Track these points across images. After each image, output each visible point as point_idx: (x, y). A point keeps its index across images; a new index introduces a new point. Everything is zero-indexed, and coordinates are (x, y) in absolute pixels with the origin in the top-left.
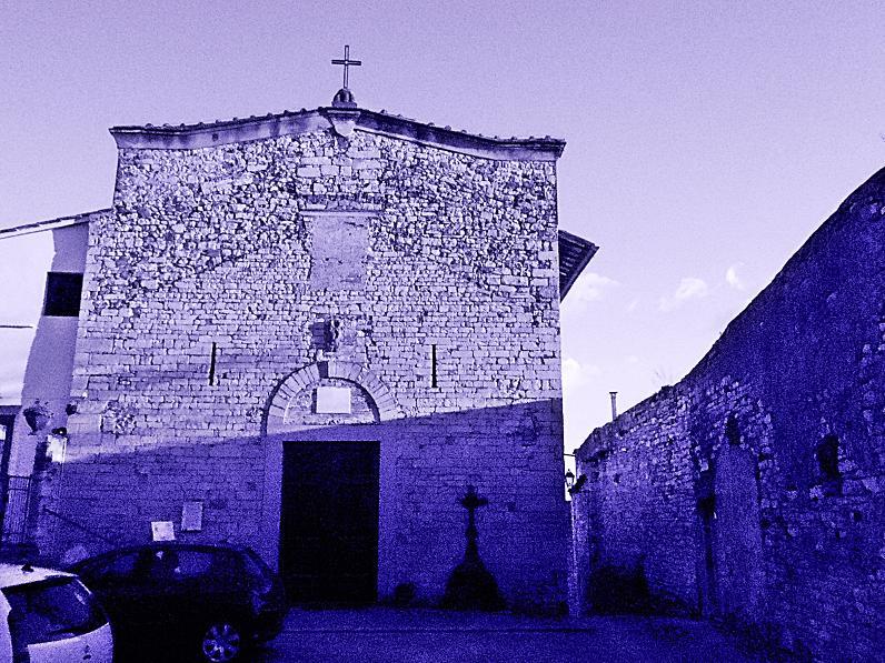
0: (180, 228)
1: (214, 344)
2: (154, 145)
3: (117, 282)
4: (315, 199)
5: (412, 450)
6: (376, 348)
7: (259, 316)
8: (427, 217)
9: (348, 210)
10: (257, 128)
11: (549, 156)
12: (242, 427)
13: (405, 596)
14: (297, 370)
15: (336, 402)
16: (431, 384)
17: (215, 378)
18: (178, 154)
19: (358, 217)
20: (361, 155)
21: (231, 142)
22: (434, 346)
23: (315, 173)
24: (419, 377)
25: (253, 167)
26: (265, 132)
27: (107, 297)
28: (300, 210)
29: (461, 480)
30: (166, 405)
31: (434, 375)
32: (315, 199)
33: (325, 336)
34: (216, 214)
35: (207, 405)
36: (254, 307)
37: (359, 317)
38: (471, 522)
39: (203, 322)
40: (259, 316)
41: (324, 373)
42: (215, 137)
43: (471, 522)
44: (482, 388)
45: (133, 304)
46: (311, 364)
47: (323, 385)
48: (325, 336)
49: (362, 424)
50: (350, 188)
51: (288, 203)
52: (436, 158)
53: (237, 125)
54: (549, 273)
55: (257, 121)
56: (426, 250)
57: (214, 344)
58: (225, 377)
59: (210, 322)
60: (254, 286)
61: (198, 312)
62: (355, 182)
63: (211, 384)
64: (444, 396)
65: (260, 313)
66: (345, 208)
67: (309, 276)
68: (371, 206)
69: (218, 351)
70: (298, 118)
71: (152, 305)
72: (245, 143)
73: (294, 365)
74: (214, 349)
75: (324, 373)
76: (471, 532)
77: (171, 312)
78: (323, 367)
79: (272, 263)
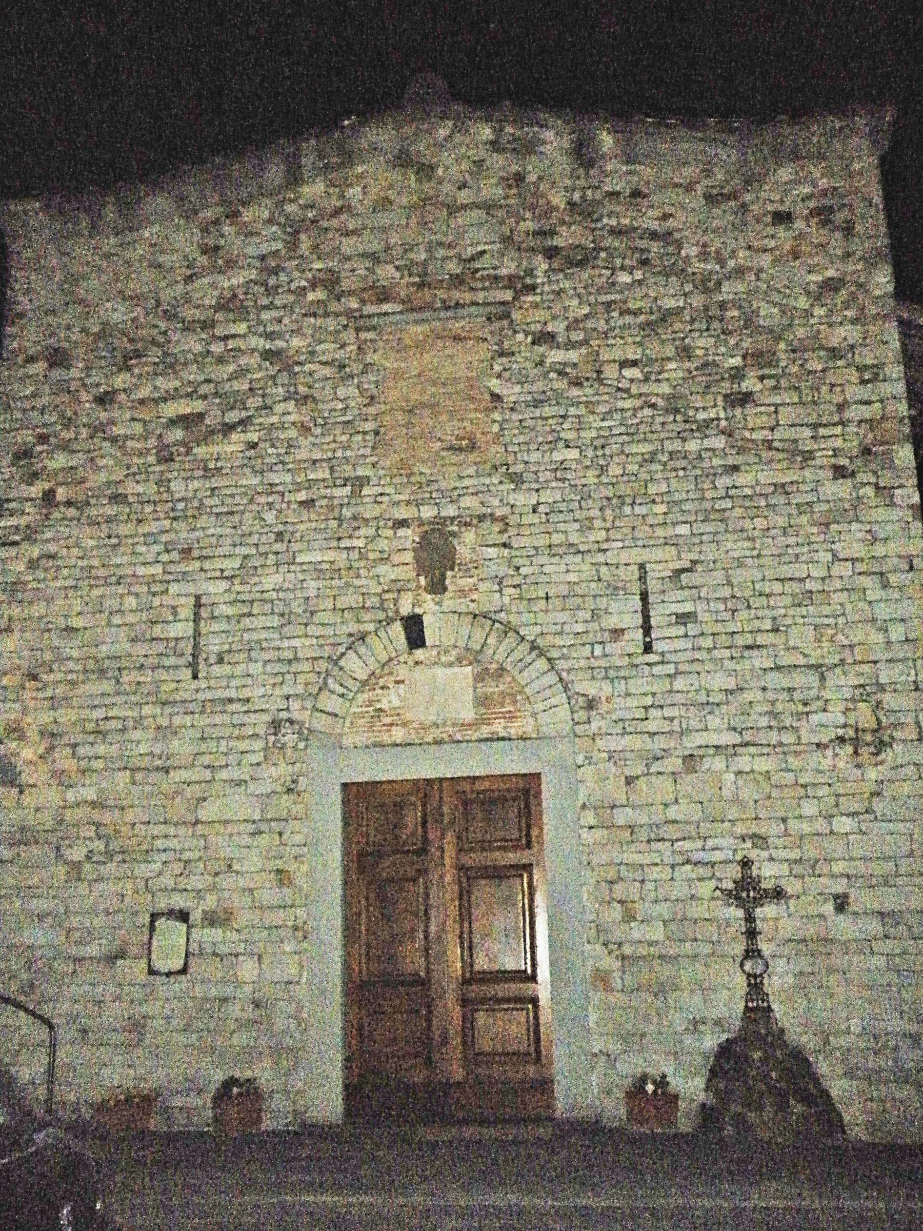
0: (121, 380)
1: (198, 598)
5: (616, 791)
7: (280, 536)
9: (447, 308)
14: (363, 637)
17: (202, 666)
20: (464, 197)
22: (642, 566)
24: (617, 633)
30: (114, 724)
35: (188, 720)
37: (481, 518)
39: (175, 556)
46: (390, 621)
49: (503, 739)
54: (887, 389)
56: (611, 372)
58: (220, 661)
59: (186, 552)
61: (164, 538)
65: (281, 527)
69: (204, 613)
73: (353, 628)
77: (114, 541)
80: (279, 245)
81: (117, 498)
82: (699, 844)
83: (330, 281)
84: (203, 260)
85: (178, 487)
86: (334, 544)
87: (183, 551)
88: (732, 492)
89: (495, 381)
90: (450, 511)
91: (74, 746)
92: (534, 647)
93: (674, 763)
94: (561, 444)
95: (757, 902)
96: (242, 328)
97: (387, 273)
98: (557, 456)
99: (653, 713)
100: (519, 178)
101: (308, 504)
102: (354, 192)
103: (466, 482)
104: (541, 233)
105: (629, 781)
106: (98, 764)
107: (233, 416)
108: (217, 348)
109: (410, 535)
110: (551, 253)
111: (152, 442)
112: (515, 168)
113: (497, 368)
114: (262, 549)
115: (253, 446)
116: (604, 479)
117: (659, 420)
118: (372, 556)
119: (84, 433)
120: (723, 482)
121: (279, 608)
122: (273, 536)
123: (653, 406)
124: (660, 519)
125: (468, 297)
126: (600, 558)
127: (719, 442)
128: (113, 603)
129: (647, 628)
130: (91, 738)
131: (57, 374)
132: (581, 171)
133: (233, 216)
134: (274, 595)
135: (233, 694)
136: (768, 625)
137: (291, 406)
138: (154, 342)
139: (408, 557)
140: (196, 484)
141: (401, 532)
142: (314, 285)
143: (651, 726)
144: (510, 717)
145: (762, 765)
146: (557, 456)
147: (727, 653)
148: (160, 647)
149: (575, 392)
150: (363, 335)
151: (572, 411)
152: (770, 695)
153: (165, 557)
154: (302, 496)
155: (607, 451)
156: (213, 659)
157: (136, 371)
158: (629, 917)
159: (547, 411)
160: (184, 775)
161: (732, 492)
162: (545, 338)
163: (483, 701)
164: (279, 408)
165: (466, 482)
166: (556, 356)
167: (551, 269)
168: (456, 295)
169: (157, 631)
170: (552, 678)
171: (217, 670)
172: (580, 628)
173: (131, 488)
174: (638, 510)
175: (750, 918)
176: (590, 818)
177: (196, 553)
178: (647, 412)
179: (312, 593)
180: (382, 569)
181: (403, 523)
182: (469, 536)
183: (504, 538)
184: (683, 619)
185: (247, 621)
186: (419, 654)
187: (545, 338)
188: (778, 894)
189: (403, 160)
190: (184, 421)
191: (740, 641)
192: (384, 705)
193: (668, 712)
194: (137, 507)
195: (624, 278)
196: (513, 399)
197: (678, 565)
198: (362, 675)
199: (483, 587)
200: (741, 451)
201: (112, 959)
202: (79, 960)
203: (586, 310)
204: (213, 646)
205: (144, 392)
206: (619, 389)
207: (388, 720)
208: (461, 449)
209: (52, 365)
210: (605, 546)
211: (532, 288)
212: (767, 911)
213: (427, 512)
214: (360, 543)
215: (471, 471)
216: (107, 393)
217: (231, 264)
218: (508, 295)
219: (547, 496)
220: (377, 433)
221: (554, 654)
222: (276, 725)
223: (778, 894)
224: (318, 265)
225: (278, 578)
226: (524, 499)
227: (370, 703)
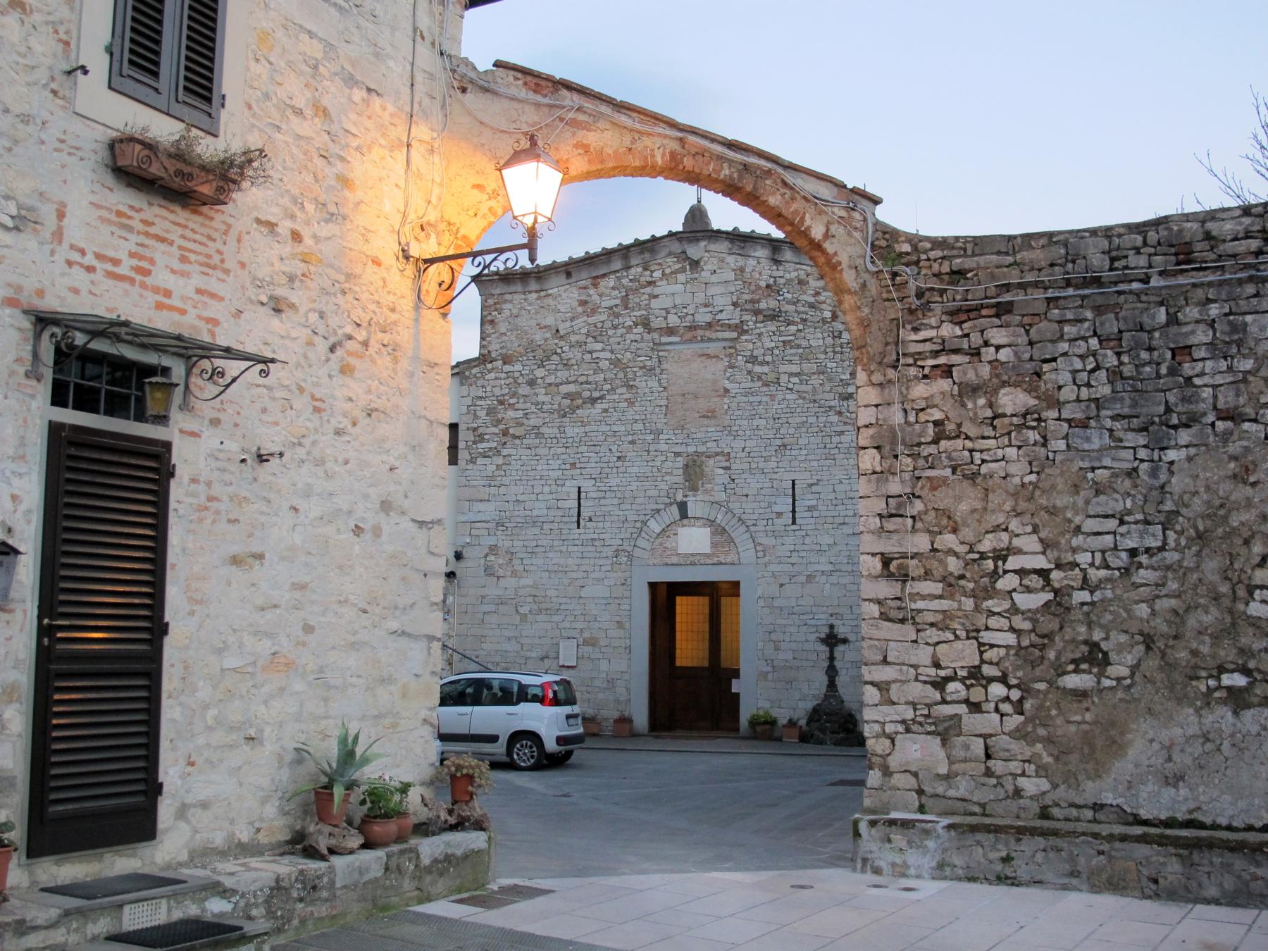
0: (540, 373)
1: (579, 488)
2: (512, 288)
3: (488, 431)
4: (671, 331)
5: (775, 589)
6: (734, 486)
8: (783, 342)
9: (702, 341)
10: (608, 262)
12: (609, 568)
13: (765, 729)
14: (658, 511)
15: (694, 539)
16: (790, 521)
17: (581, 521)
18: (535, 295)
19: (713, 348)
20: (714, 279)
21: (584, 276)
22: (793, 481)
23: (668, 303)
24: (779, 515)
25: (607, 303)
26: (617, 265)
27: (479, 445)
28: (654, 344)
29: (823, 619)
30: (539, 549)
31: (794, 511)
32: (671, 331)
33: (693, 472)
34: (574, 355)
36: (614, 448)
37: (717, 454)
38: (832, 658)
39: (568, 466)
40: (619, 458)
41: (684, 514)
42: (569, 275)
43: (832, 658)
44: (844, 523)
45: (505, 452)
46: (671, 504)
47: (683, 526)
48: (693, 472)
50: (703, 317)
51: (642, 338)
52: (794, 274)
53: (589, 260)
55: (607, 254)
56: (784, 378)
57: (579, 488)
58: (590, 520)
59: (573, 465)
60: (615, 428)
61: (563, 457)
62: (710, 309)
63: (578, 527)
64: (803, 533)
66: (699, 338)
67: (666, 415)
69: (583, 495)
70: (648, 246)
71: (521, 451)
72: (597, 277)
73: (655, 506)
74: (579, 492)
75: (684, 514)
76: (832, 672)
77: (538, 458)
78: (683, 507)
79: (631, 403)
80: (618, 301)
81: (539, 435)
82: (811, 616)
83: (646, 323)
84: (580, 309)
85: (569, 431)
86: (646, 464)
87: (571, 464)
88: (839, 445)
89: (727, 382)
90: (701, 449)
91: (522, 559)
92: (740, 519)
93: (803, 579)
94: (757, 417)
95: (835, 644)
96: (599, 346)
97: (673, 320)
98: (755, 423)
99: (794, 554)
100: (742, 270)
101: (632, 442)
102: (657, 274)
103: (709, 435)
104: (753, 301)
105: (781, 585)
106: (532, 568)
107: (596, 394)
108: (587, 357)
109: (681, 461)
110: (757, 312)
111: (555, 407)
112: (739, 264)
113: (728, 375)
114: (611, 465)
115: (605, 411)
116: (778, 436)
117: (806, 406)
118: (664, 470)
119: (521, 400)
120: (836, 439)
121: (619, 494)
122: (615, 459)
123: (804, 398)
124: (804, 458)
125: (713, 336)
126: (775, 476)
127: (835, 418)
128: (537, 490)
129: (794, 511)
130: (530, 555)
131: (507, 368)
132: (775, 267)
133: (595, 285)
134: (616, 489)
135: (596, 536)
136: (851, 513)
137: (624, 390)
138: (556, 353)
139: (681, 472)
140: (577, 430)
141: (678, 459)
142: (636, 325)
143: (793, 560)
144: (727, 553)
145: (844, 581)
146: (755, 423)
147: (831, 526)
148: (560, 513)
149: (765, 389)
150: (661, 354)
151: (764, 399)
152: (849, 548)
153: (563, 467)
154: (630, 438)
155: (781, 421)
156: (587, 519)
157: (547, 367)
158: (777, 649)
159: (751, 399)
160: (574, 575)
161: (839, 445)
162: (753, 360)
163: (714, 545)
164: (618, 391)
165: (709, 435)
166: (758, 369)
167: (756, 322)
168: (708, 334)
169: (560, 504)
170: (748, 535)
171: (589, 524)
172: (762, 511)
173: (545, 430)
174: (794, 453)
175: (832, 652)
176: (761, 603)
177: (578, 466)
178: (801, 401)
179: (634, 488)
180: (667, 478)
181: (678, 454)
182: (712, 461)
183: (727, 464)
184: (811, 509)
185: (603, 502)
186: (685, 521)
187: (753, 360)
188: (845, 641)
190: (571, 396)
191: (838, 520)
192: (667, 545)
193: (804, 554)
194: (549, 441)
195: (793, 328)
196: (734, 391)
197: (811, 482)
198: (658, 529)
199: (716, 488)
200: (846, 423)
201: (542, 659)
202: (527, 659)
203: (773, 344)
204: (585, 513)
205: (551, 379)
206: (788, 389)
207: (669, 553)
208: (708, 417)
209: (505, 363)
210: (776, 470)
211: (747, 331)
212: (840, 649)
213: (691, 449)
214: (658, 464)
215: (713, 429)
216: (532, 379)
217: (594, 311)
218: (734, 335)
219: (749, 443)
220: (667, 406)
221: (750, 523)
222: (617, 553)
223: (845, 641)
224: (638, 314)
225: (618, 480)
226: (738, 444)
227: (661, 544)
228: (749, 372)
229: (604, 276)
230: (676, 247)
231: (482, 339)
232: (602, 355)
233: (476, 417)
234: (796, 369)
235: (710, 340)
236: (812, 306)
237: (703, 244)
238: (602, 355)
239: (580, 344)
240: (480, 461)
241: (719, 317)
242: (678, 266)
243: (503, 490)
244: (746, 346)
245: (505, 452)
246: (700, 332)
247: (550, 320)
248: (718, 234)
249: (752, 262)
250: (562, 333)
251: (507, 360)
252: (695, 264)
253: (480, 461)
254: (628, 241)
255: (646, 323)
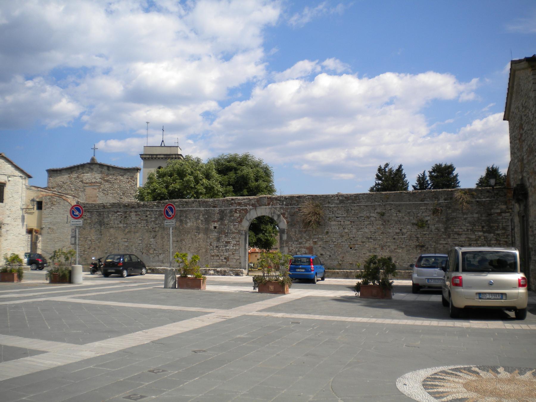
11: (136, 171)
19: (95, 187)
23: (86, 177)
26: (76, 169)
32: (87, 183)
45: (52, 207)
50: (94, 181)
68: (98, 185)
70: (83, 166)
83: (82, 181)
96: (72, 186)
97: (87, 181)
166: (104, 192)
187: (103, 190)
189: (90, 168)
228: (103, 193)
229: (73, 171)
230: (88, 166)
231: (48, 183)
232: (72, 188)
233: (46, 200)
234: (112, 192)
235: (95, 186)
236: (115, 179)
237: (94, 165)
238: (72, 188)
239: (68, 185)
240: (47, 209)
241: (97, 181)
242: (88, 170)
243: (51, 216)
244: (102, 186)
245: (52, 207)
246: (93, 184)
247: (62, 180)
248: (97, 164)
249: (103, 170)
250: (64, 183)
251: (53, 188)
252: (92, 169)
253: (47, 209)
254: (79, 164)
255: (82, 181)
